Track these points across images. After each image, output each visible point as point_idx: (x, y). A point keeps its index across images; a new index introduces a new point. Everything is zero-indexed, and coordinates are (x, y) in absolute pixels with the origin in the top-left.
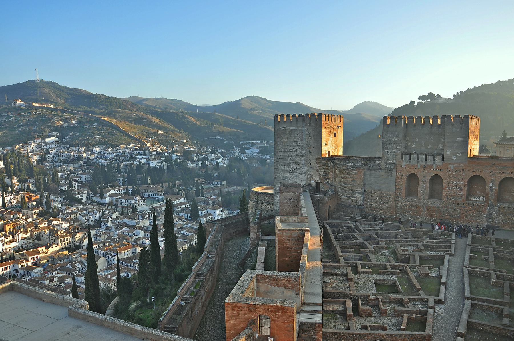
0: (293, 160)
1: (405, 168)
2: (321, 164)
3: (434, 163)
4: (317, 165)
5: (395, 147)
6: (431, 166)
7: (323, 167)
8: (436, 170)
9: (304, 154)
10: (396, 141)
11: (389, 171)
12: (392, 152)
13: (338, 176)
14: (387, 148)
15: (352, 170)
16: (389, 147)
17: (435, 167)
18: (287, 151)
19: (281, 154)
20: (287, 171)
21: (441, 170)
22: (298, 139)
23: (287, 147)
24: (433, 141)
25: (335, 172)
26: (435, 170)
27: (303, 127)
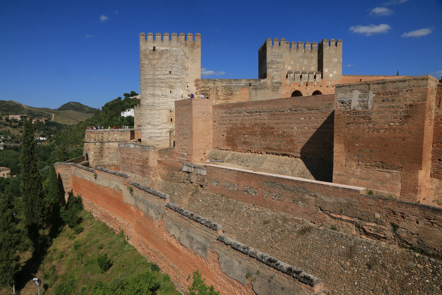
0: (166, 83)
1: (290, 86)
2: (201, 86)
3: (315, 81)
4: (195, 88)
5: (280, 67)
6: (312, 83)
7: (203, 89)
8: (317, 86)
9: (179, 76)
10: (280, 61)
11: (274, 89)
12: (277, 71)
13: (221, 98)
14: (271, 68)
15: (235, 91)
16: (274, 66)
17: (315, 84)
18: (157, 73)
19: (150, 77)
20: (158, 96)
21: (320, 86)
22: (171, 60)
23: (158, 69)
24: (306, 64)
25: (217, 93)
26: (316, 86)
27: (178, 47)
